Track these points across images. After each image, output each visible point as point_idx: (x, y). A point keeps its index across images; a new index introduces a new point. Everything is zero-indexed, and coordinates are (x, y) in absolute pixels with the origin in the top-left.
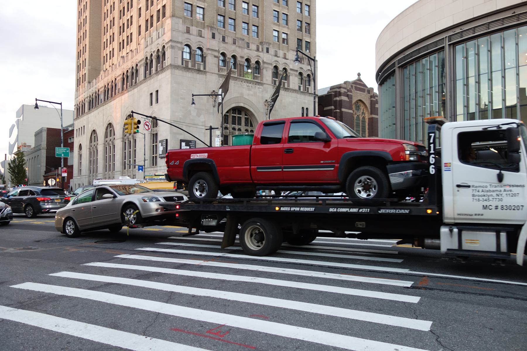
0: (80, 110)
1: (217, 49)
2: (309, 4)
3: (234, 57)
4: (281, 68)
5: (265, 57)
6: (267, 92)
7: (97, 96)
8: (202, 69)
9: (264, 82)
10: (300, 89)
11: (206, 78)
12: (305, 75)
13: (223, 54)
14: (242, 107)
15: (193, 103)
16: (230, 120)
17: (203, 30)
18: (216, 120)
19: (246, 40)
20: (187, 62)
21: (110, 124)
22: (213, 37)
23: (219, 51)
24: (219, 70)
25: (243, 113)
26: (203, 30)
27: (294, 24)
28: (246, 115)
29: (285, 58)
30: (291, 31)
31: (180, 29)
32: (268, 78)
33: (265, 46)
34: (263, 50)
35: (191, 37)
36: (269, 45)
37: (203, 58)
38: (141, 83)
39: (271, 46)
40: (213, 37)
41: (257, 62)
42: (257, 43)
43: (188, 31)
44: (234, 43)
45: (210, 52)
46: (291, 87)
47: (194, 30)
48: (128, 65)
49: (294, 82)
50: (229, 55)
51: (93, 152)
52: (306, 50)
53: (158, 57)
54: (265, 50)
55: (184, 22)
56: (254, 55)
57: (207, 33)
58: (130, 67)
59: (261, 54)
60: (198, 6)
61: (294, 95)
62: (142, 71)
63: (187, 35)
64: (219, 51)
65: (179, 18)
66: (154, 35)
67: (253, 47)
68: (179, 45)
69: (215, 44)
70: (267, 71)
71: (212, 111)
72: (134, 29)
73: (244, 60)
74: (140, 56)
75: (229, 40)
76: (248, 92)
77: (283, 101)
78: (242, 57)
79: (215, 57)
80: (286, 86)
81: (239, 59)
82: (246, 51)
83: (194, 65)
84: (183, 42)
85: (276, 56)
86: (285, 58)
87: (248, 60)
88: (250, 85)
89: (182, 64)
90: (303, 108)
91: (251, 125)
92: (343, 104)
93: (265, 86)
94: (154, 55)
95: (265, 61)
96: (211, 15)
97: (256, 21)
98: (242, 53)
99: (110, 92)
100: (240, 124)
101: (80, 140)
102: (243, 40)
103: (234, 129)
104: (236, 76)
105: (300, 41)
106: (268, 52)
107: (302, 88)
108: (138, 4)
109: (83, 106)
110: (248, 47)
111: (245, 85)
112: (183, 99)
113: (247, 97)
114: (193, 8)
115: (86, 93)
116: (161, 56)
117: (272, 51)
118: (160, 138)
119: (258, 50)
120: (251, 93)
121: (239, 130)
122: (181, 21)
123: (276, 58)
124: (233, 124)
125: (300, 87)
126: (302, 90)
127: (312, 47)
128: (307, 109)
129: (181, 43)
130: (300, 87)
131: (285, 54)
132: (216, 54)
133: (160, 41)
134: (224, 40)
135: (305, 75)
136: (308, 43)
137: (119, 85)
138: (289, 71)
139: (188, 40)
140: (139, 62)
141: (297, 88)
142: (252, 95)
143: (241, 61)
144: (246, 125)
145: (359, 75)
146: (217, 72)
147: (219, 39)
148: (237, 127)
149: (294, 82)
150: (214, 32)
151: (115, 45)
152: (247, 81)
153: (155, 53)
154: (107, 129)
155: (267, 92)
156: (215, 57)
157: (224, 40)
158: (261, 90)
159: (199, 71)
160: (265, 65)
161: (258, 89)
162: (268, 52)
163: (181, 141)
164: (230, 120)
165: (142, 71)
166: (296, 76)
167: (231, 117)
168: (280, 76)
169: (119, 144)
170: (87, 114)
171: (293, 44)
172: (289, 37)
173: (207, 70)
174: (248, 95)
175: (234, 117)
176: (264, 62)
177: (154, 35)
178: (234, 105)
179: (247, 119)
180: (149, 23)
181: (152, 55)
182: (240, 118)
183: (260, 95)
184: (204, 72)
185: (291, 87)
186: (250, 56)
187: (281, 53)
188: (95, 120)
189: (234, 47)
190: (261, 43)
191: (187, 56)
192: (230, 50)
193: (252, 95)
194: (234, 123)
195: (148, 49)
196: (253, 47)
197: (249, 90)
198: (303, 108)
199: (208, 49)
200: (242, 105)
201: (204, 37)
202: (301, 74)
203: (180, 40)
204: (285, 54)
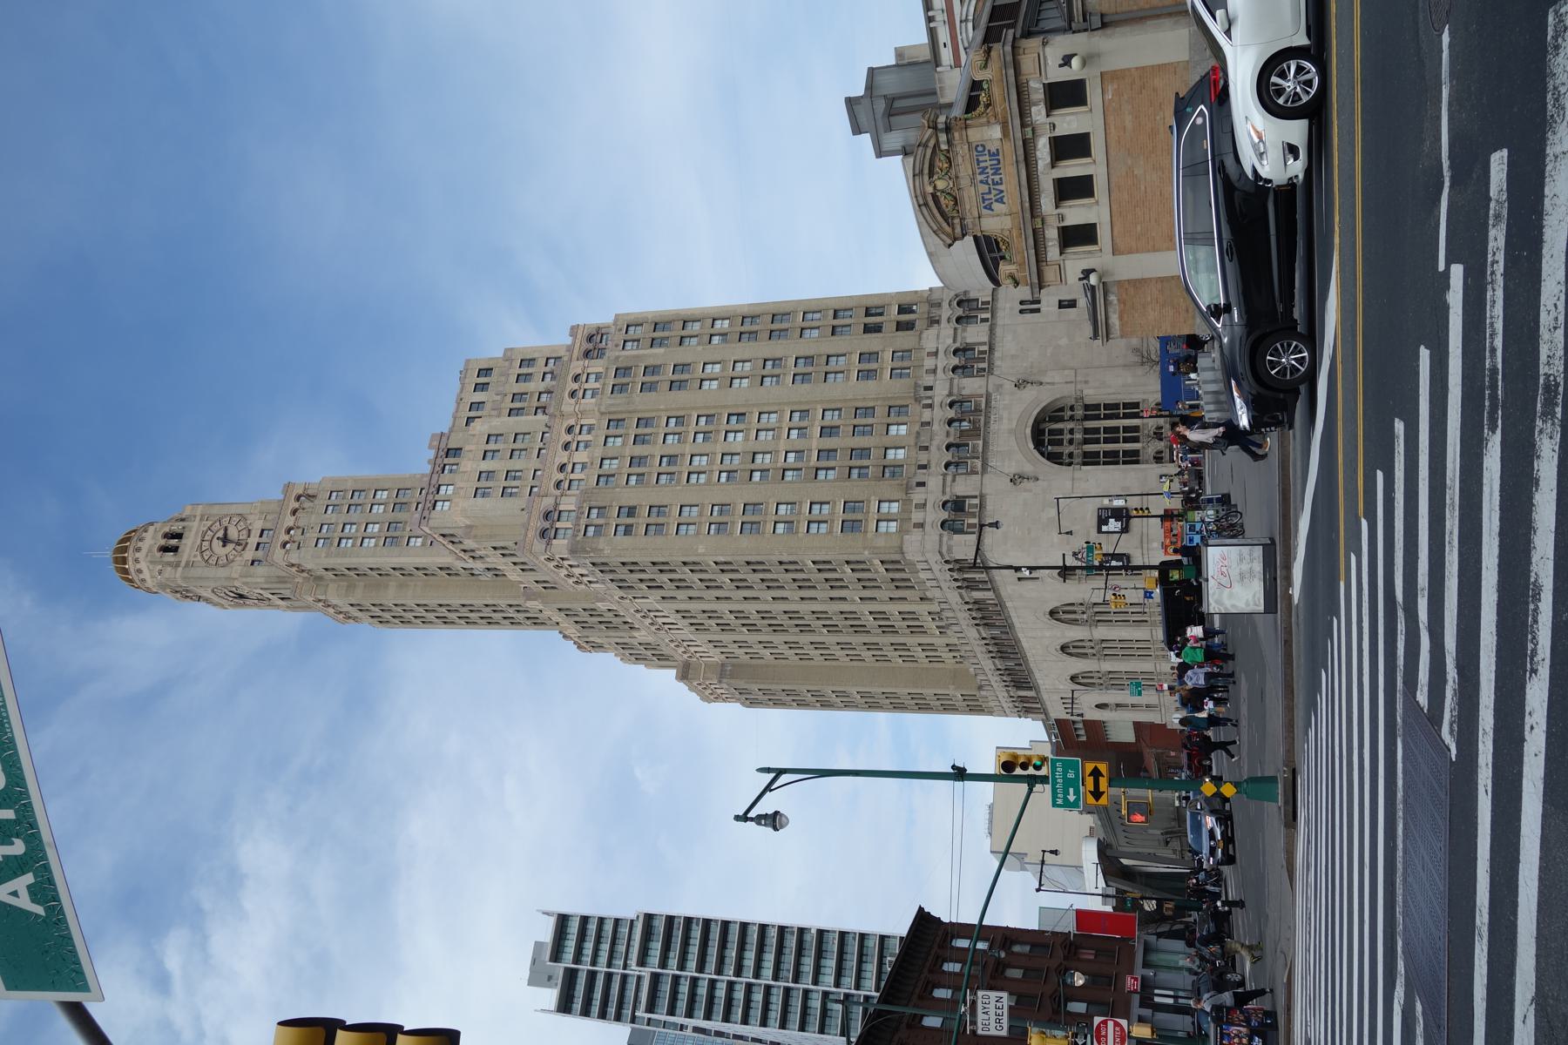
0: (1028, 706)
2: (831, 313)
3: (948, 447)
4: (955, 361)
5: (940, 393)
7: (1009, 671)
8: (976, 501)
9: (983, 391)
10: (986, 320)
12: (960, 312)
13: (947, 466)
15: (1070, 533)
16: (1057, 449)
18: (1060, 479)
19: (917, 427)
20: (970, 526)
21: (1063, 648)
22: (922, 484)
24: (974, 472)
25: (1042, 426)
27: (872, 342)
29: (936, 354)
30: (886, 344)
33: (923, 393)
35: (929, 521)
38: (998, 596)
40: (922, 484)
41: (951, 405)
42: (918, 408)
43: (921, 525)
44: (926, 448)
47: (917, 516)
48: (964, 617)
49: (975, 334)
50: (948, 457)
51: (1112, 681)
52: (913, 312)
53: (960, 570)
54: (929, 393)
55: (908, 532)
57: (918, 496)
58: (967, 614)
59: (937, 400)
61: (999, 331)
62: (977, 595)
63: (927, 527)
64: (944, 475)
66: (923, 575)
67: (926, 415)
69: (934, 483)
72: (893, 609)
73: (952, 430)
74: (954, 597)
75: (923, 458)
78: (948, 434)
80: (986, 348)
81: (951, 440)
82: (935, 427)
83: (973, 515)
85: (934, 371)
86: (936, 354)
87: (950, 422)
90: (1021, 312)
91: (1062, 409)
94: (956, 575)
96: (888, 488)
97: (881, 411)
98: (940, 435)
99: (1006, 649)
100: (1061, 432)
101: (1088, 705)
103: (1071, 442)
104: (980, 442)
105: (900, 326)
106: (930, 388)
107: (984, 316)
108: (766, 602)
109: (1023, 699)
110: (928, 424)
111: (993, 427)
115: (998, 690)
116: (959, 566)
117: (928, 380)
119: (930, 406)
120: (1005, 415)
121: (1071, 431)
123: (939, 371)
125: (983, 320)
126: (988, 315)
127: (907, 300)
128: (1022, 303)
130: (983, 320)
131: (929, 354)
132: (949, 478)
133: (936, 568)
134: (924, 467)
135: (960, 312)
136: (902, 310)
137: (996, 632)
138: (958, 345)
144: (1061, 420)
146: (976, 478)
148: (1067, 437)
149: (975, 334)
151: (912, 641)
152: (987, 423)
154: (1070, 654)
157: (924, 467)
159: (982, 506)
160: (955, 391)
161: (999, 402)
162: (930, 388)
163: (1100, 531)
164: (1057, 449)
165: (977, 595)
166: (964, 330)
168: (968, 360)
169: (1101, 632)
170: (1038, 692)
171: (905, 340)
172: (898, 346)
175: (1051, 443)
176: (950, 394)
177: (923, 575)
180: (899, 584)
182: (1051, 432)
184: (982, 497)
185: (986, 339)
187: (929, 363)
188: (1052, 676)
189: (933, 448)
190: (917, 400)
194: (1060, 443)
195: (943, 585)
196: (927, 412)
197: (1001, 419)
198: (1021, 312)
199: (944, 492)
200: (1029, 431)
202: (958, 320)
204: (929, 354)
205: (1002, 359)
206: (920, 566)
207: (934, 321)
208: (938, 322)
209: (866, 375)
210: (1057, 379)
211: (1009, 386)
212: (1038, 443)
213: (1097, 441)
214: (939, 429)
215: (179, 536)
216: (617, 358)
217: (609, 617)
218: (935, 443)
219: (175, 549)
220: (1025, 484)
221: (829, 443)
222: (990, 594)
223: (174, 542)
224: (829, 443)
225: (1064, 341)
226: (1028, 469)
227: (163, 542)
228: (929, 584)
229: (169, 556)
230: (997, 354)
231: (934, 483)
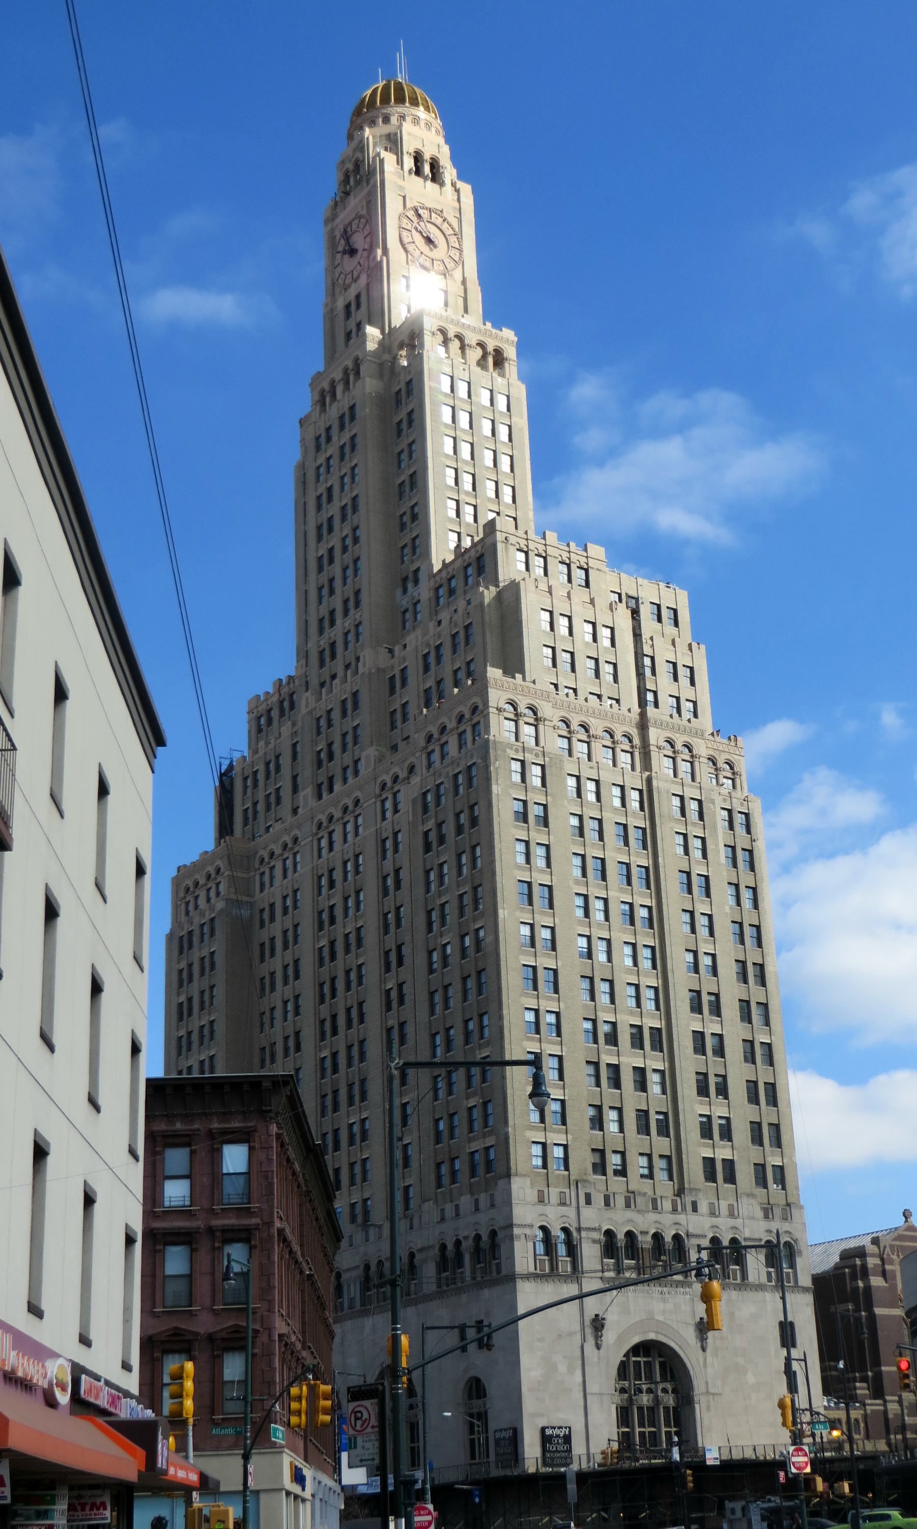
1: (597, 1225)
28: (660, 1356)
31: (528, 1199)
34: (684, 1209)
36: (697, 1195)
37: (572, 1250)
38: (429, 1298)
39: (700, 1195)
40: (588, 1201)
41: (677, 1237)
44: (628, 1206)
46: (752, 1277)
54: (689, 1207)
59: (681, 1218)
60: (555, 1144)
63: (540, 1208)
65: (524, 1176)
68: (528, 1231)
71: (596, 1359)
76: (661, 1306)
79: (594, 1241)
82: (653, 1216)
85: (713, 1214)
86: (732, 1214)
87: (657, 1237)
88: (665, 1289)
89: (536, 1269)
92: (876, 1296)
94: (467, 1245)
95: (691, 1231)
98: (644, 1223)
102: (645, 1194)
110: (655, 1208)
112: (541, 1340)
113: (661, 1318)
114: (548, 1151)
117: (703, 1207)
118: (492, 1426)
119: (675, 1210)
120: (669, 1306)
123: (715, 1221)
124: (636, 1379)
125: (769, 1274)
129: (531, 1226)
134: (607, 1204)
139: (543, 1217)
140: (421, 1250)
141: (764, 1279)
143: (645, 1241)
145: (906, 1214)
153: (471, 1241)
156: (594, 1241)
158: (688, 1297)
162: (695, 1209)
167: (632, 1364)
168: (726, 1255)
171: (745, 1174)
174: (664, 1312)
177: (465, 1201)
178: (636, 1340)
179: (662, 1365)
181: (458, 1243)
189: (630, 1214)
191: (540, 1249)
192: (621, 1221)
196: (667, 1205)
197: (664, 1301)
200: (652, 1336)
203: (528, 1222)
206: (483, 1198)
207: (767, 1212)
208: (766, 1217)
209: (706, 1131)
210: (710, 1370)
212: (637, 1349)
213: (642, 1425)
215: (436, 176)
216: (713, 802)
217: (341, 759)
219: (418, 172)
221: (627, 1079)
222: (430, 1287)
223: (427, 169)
224: (627, 1079)
225: (751, 1379)
227: (427, 156)
228: (449, 1209)
229: (409, 163)
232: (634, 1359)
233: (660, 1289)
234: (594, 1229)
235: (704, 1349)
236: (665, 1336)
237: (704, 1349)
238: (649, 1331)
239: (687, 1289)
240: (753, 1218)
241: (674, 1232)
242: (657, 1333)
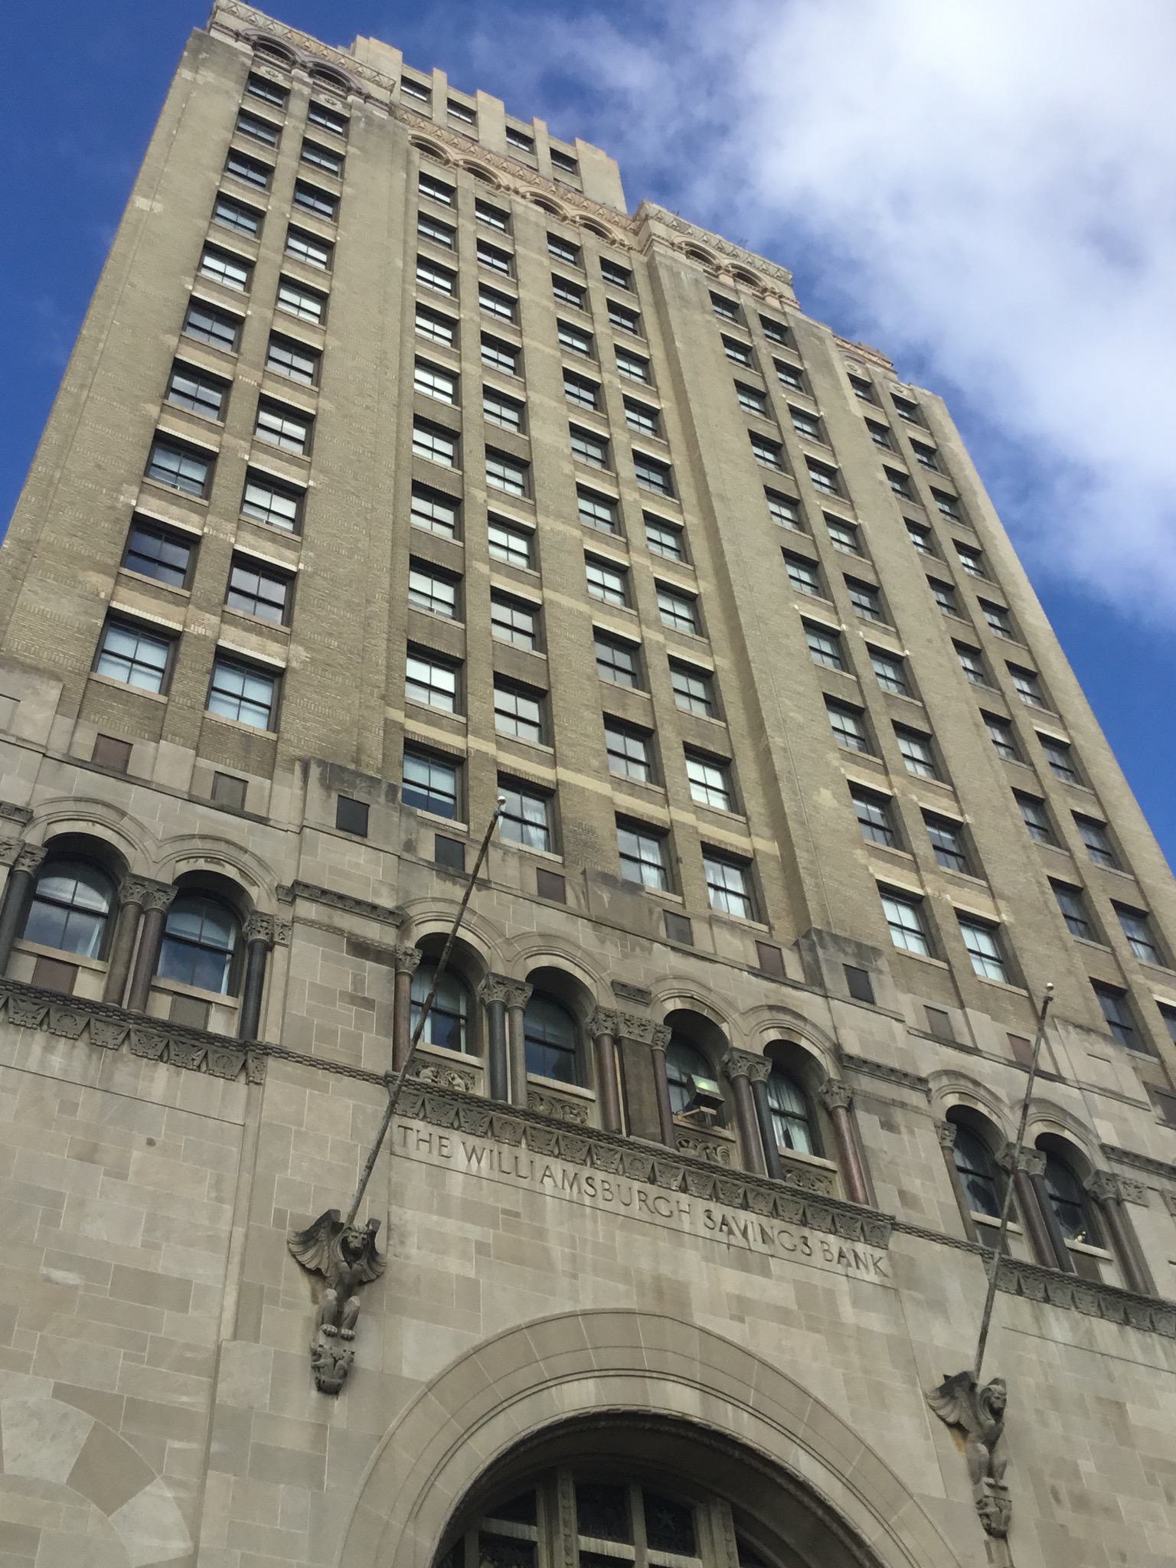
1: (387, 902)
6: (938, 1305)
9: (888, 1203)
11: (251, 1106)
14: (680, 1425)
17: (254, 780)
23: (399, 919)
26: (254, 780)
32: (915, 1184)
35: (133, 798)
40: (353, 821)
43: (112, 759)
45: (307, 909)
47: (168, 761)
54: (837, 983)
56: (745, 1002)
64: (399, 919)
70: (888, 1125)
76: (732, 1280)
77: (1135, 1413)
79: (361, 948)
82: (667, 961)
84: (40, 812)
88: (743, 1216)
93: (898, 1242)
95: (852, 1047)
111: (693, 1211)
113: (734, 1332)
120: (774, 1289)
122: (53, 693)
139: (100, 810)
142: (783, 1316)
147: (410, 846)
150: (360, 795)
155: (938, 1305)
156: (361, 948)
159: (182, 1043)
173: (270, 1033)
174: (742, 1308)
183: (875, 1322)
186: (711, 999)
189: (550, 918)
193: (783, 1316)
197: (743, 1259)
199: (295, 891)
201: (263, 821)
205: (1087, 1347)
211: (950, 1344)
214: (669, 976)
218: (582, 933)
220: (297, 1306)
226: (409, 1346)
230: (1105, 1331)
231: (359, 867)
232: (590, 1544)
233: (718, 1210)
234: (371, 910)
235: (998, 1533)
236: (757, 1413)
237: (998, 1533)
238: (663, 1376)
239: (861, 1248)
240: (1119, 1097)
241: (773, 1035)
242: (705, 1389)
